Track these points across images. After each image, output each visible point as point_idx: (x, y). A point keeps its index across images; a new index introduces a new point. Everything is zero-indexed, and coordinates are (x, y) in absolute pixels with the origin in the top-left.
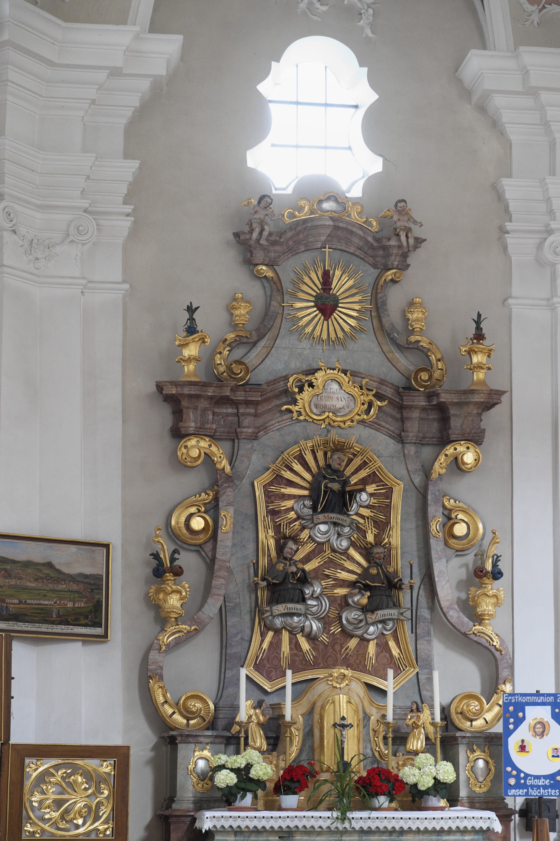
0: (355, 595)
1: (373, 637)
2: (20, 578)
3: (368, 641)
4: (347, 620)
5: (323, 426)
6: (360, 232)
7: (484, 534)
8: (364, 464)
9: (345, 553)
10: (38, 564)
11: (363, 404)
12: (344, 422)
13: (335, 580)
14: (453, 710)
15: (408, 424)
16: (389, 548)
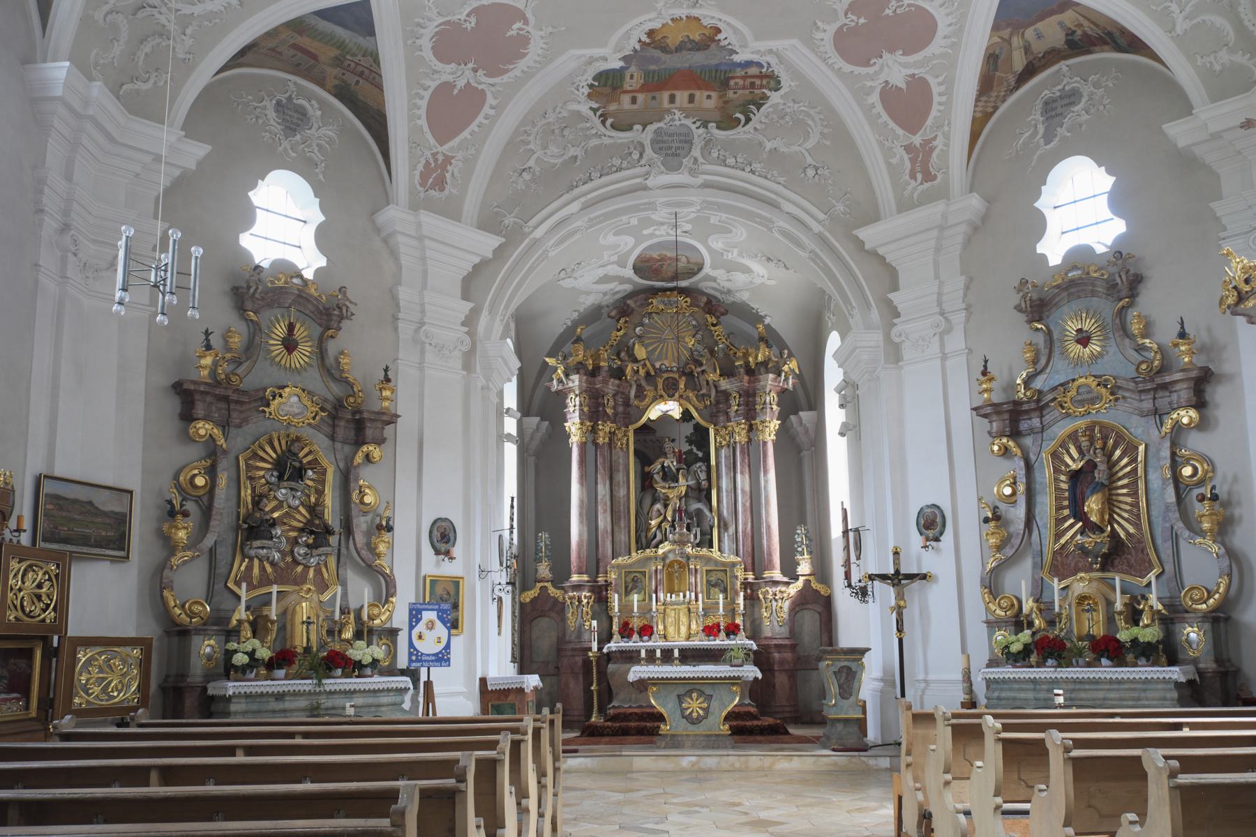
0: (303, 536)
2: (69, 512)
3: (309, 567)
6: (315, 302)
8: (310, 452)
9: (296, 508)
10: (82, 502)
13: (289, 526)
15: (337, 429)
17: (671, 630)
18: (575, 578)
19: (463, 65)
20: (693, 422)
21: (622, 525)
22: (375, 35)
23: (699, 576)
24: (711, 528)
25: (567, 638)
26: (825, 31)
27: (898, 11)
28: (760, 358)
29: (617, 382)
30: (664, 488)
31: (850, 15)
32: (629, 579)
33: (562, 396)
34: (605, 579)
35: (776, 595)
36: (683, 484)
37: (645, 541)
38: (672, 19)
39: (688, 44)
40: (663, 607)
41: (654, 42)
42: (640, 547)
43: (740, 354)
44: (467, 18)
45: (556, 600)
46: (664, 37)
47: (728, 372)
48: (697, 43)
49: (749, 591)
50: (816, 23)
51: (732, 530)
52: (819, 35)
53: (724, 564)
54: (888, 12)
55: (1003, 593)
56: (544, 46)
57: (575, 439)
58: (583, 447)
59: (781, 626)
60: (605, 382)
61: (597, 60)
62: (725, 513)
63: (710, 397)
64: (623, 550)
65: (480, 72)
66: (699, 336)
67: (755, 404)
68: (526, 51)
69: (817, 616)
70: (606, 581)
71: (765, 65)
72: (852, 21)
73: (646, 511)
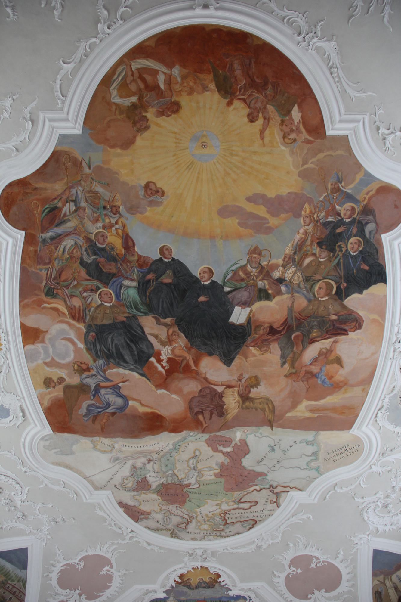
19: (73, 591)
22: (27, 569)
26: (279, 577)
27: (318, 565)
31: (292, 568)
38: (193, 568)
39: (203, 583)
41: (183, 582)
44: (79, 562)
46: (189, 579)
48: (207, 584)
50: (273, 573)
52: (276, 580)
54: (313, 566)
56: (121, 582)
61: (150, 592)
65: (83, 596)
68: (110, 585)
71: (248, 598)
72: (294, 571)
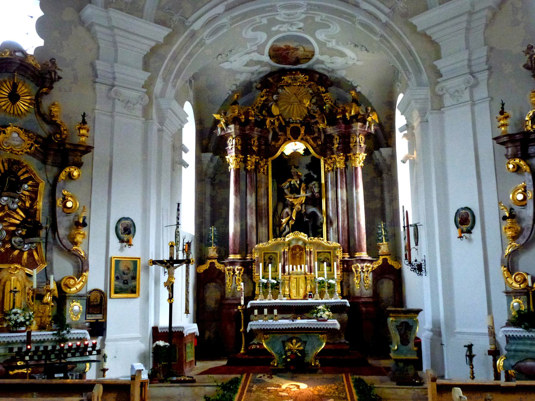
1: (27, 249)
4: (15, 242)
5: (8, 152)
7: (79, 207)
11: (28, 145)
12: (19, 152)
14: (62, 284)
16: (36, 210)
17: (294, 291)
18: (231, 257)
20: (311, 156)
21: (264, 221)
23: (312, 256)
24: (322, 224)
25: (226, 296)
28: (353, 113)
29: (260, 129)
30: (291, 198)
32: (267, 257)
33: (223, 140)
34: (251, 257)
35: (363, 269)
36: (303, 195)
37: (278, 233)
40: (288, 276)
42: (276, 236)
43: (340, 111)
45: (220, 271)
47: (332, 122)
49: (345, 266)
51: (335, 225)
53: (329, 248)
55: (518, 271)
57: (232, 167)
58: (237, 171)
59: (366, 289)
60: (252, 130)
62: (331, 214)
63: (321, 139)
64: (264, 239)
66: (314, 101)
67: (349, 142)
69: (391, 282)
70: (251, 259)
73: (279, 212)
